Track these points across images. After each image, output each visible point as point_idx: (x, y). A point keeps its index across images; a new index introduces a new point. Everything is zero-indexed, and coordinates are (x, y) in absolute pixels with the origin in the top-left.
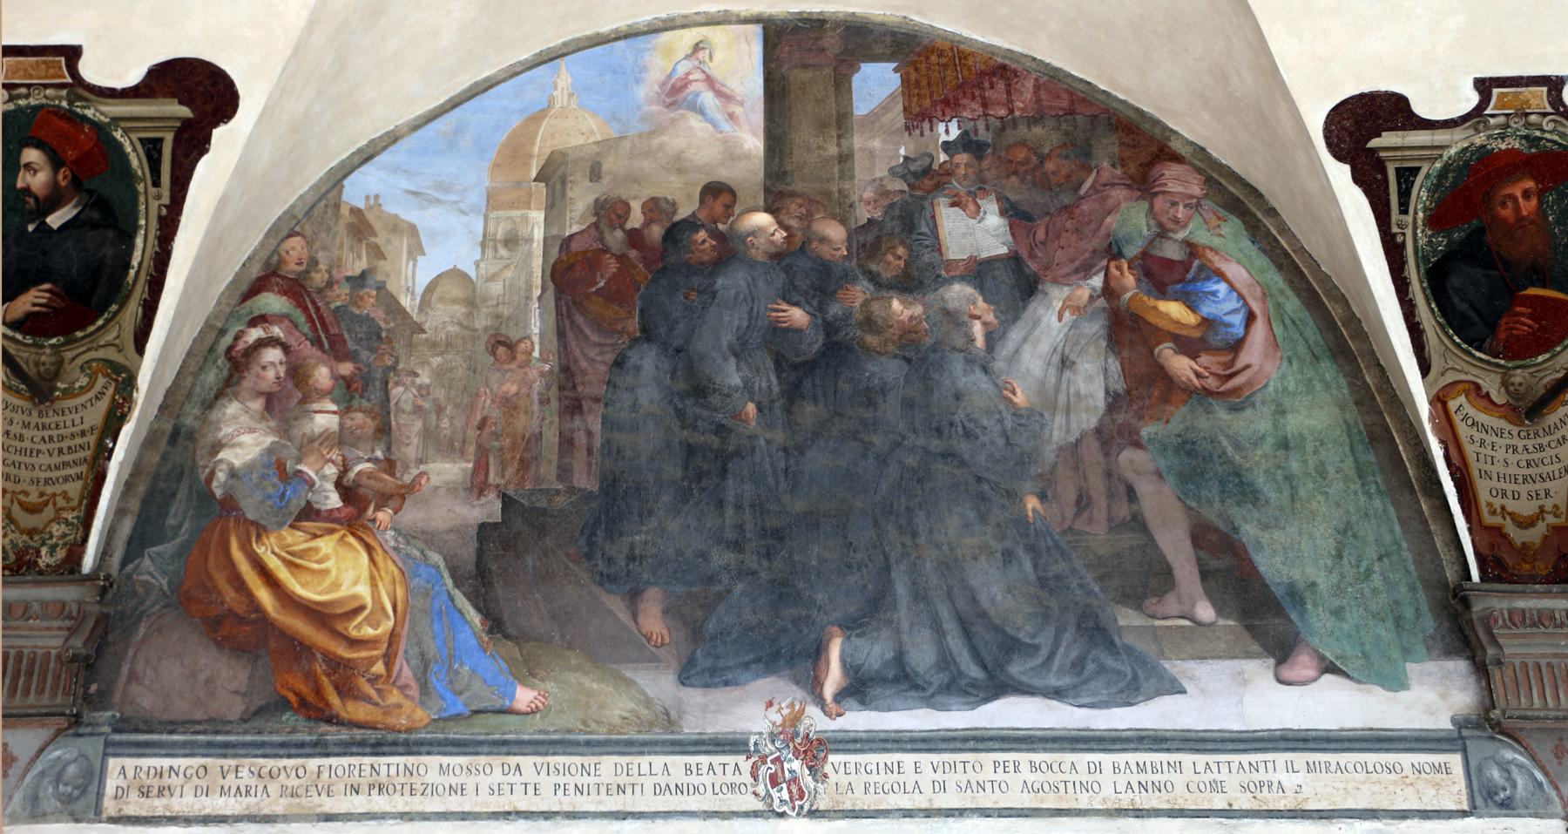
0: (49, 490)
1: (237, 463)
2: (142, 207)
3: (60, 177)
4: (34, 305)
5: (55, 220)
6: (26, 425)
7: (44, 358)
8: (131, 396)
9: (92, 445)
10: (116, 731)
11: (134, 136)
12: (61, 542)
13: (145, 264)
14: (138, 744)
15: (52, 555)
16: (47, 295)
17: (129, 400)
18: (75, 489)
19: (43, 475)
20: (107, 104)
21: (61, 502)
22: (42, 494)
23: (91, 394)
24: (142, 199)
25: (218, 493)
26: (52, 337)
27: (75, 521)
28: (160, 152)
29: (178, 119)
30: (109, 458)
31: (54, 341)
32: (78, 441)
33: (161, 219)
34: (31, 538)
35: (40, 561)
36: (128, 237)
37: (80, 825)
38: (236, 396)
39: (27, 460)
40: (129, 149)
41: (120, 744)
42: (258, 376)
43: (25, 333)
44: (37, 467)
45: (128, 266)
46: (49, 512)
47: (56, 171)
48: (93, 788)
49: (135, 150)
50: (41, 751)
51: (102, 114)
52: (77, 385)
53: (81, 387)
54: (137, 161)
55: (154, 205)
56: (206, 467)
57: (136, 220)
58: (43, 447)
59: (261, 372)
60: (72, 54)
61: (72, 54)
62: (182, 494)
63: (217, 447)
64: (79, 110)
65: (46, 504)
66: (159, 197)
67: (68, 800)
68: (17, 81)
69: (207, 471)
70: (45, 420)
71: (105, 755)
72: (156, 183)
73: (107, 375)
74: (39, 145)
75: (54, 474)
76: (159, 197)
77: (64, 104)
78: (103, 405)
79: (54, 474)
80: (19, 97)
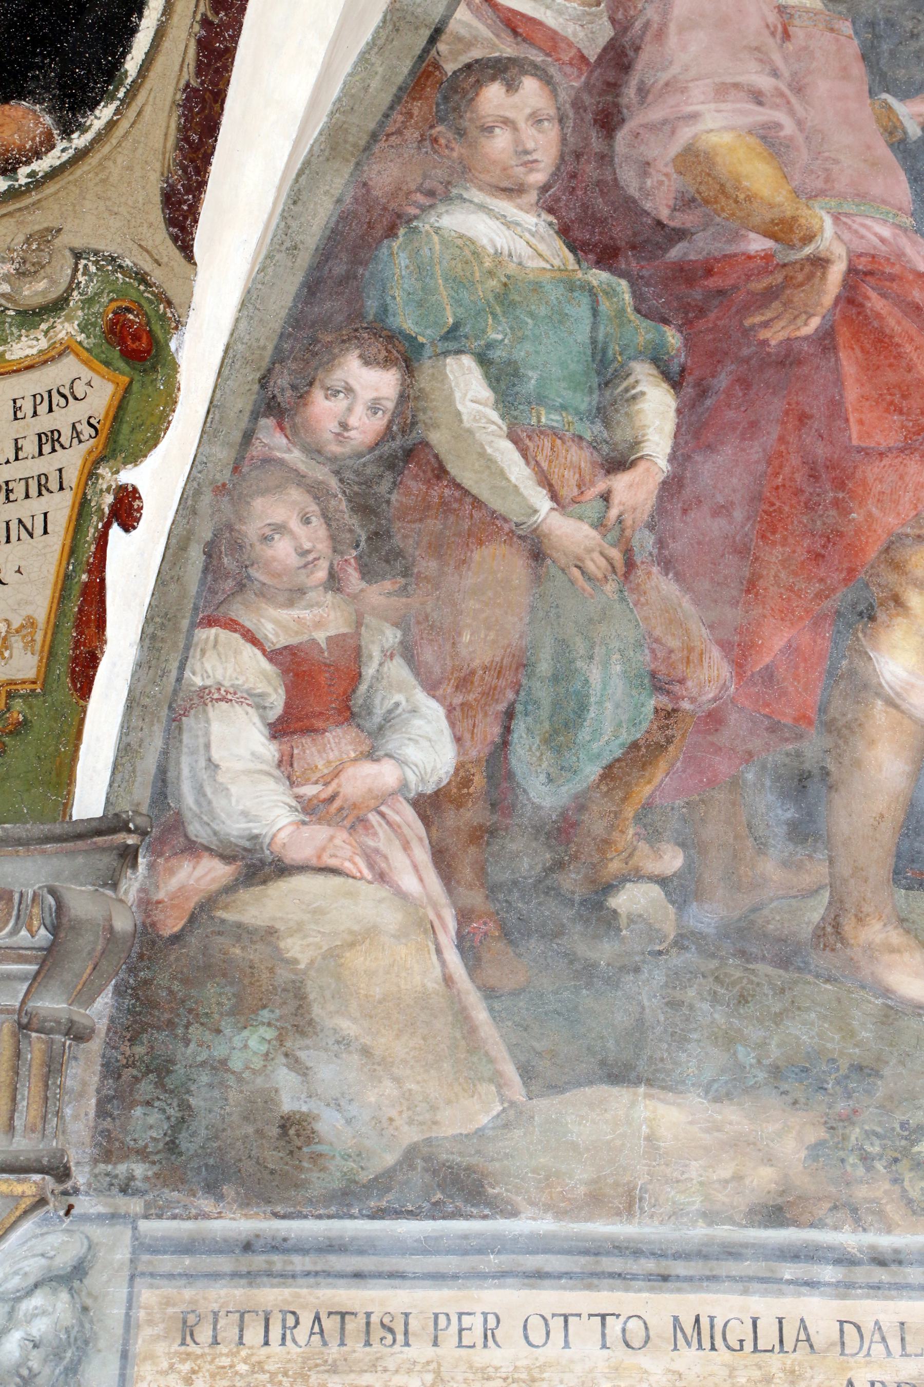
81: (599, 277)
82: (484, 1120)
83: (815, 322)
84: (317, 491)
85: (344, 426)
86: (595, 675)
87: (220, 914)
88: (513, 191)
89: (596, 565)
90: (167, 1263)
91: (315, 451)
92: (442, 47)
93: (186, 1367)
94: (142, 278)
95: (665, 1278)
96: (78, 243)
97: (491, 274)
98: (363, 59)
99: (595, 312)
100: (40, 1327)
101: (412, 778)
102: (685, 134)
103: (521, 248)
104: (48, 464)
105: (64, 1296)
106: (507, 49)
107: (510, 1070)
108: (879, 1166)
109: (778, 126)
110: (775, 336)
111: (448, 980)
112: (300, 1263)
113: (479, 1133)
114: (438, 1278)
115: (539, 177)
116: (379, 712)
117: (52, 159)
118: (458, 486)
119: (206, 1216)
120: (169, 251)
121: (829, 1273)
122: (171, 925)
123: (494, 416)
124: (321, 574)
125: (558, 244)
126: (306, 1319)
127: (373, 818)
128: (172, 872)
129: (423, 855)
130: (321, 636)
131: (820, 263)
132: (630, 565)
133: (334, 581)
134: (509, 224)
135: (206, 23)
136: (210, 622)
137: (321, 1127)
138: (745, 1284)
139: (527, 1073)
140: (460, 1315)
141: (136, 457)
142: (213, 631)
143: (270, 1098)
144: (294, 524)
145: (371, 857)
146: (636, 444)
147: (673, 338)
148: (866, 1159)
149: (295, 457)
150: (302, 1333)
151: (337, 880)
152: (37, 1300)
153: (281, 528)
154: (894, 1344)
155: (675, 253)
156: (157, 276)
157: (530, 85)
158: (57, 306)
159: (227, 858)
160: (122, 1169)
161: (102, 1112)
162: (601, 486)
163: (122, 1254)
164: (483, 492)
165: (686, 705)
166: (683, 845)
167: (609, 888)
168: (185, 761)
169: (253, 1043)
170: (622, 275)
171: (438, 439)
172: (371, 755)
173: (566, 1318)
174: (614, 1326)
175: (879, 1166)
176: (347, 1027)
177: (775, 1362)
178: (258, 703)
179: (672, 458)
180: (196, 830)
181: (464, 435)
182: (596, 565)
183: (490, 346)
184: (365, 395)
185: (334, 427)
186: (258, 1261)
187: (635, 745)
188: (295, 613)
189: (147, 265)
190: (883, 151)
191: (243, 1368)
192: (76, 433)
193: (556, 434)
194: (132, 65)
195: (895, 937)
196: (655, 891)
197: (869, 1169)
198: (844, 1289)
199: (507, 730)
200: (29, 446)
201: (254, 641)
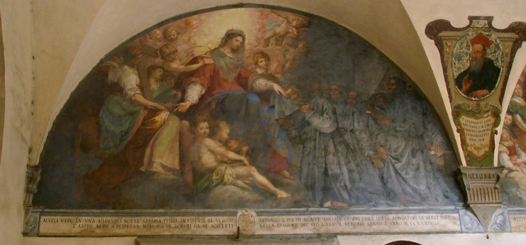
60: (490, 19)
87: (508, 176)
88: (519, 96)
94: (497, 108)
97: (519, 105)
100: (500, 219)
104: (488, 128)
105: (502, 216)
117: (488, 96)
119: (514, 208)
120: (500, 105)
123: (522, 121)
127: (521, 165)
133: (511, 139)
135: (504, 82)
143: (517, 195)
151: (518, 172)
152: (499, 216)
156: (498, 108)
158: (488, 111)
168: (500, 158)
169: (514, 189)
171: (517, 123)
172: (519, 158)
178: (506, 153)
181: (520, 123)
184: (509, 118)
189: (497, 106)
194: (496, 86)
200: (486, 126)
201: (504, 145)
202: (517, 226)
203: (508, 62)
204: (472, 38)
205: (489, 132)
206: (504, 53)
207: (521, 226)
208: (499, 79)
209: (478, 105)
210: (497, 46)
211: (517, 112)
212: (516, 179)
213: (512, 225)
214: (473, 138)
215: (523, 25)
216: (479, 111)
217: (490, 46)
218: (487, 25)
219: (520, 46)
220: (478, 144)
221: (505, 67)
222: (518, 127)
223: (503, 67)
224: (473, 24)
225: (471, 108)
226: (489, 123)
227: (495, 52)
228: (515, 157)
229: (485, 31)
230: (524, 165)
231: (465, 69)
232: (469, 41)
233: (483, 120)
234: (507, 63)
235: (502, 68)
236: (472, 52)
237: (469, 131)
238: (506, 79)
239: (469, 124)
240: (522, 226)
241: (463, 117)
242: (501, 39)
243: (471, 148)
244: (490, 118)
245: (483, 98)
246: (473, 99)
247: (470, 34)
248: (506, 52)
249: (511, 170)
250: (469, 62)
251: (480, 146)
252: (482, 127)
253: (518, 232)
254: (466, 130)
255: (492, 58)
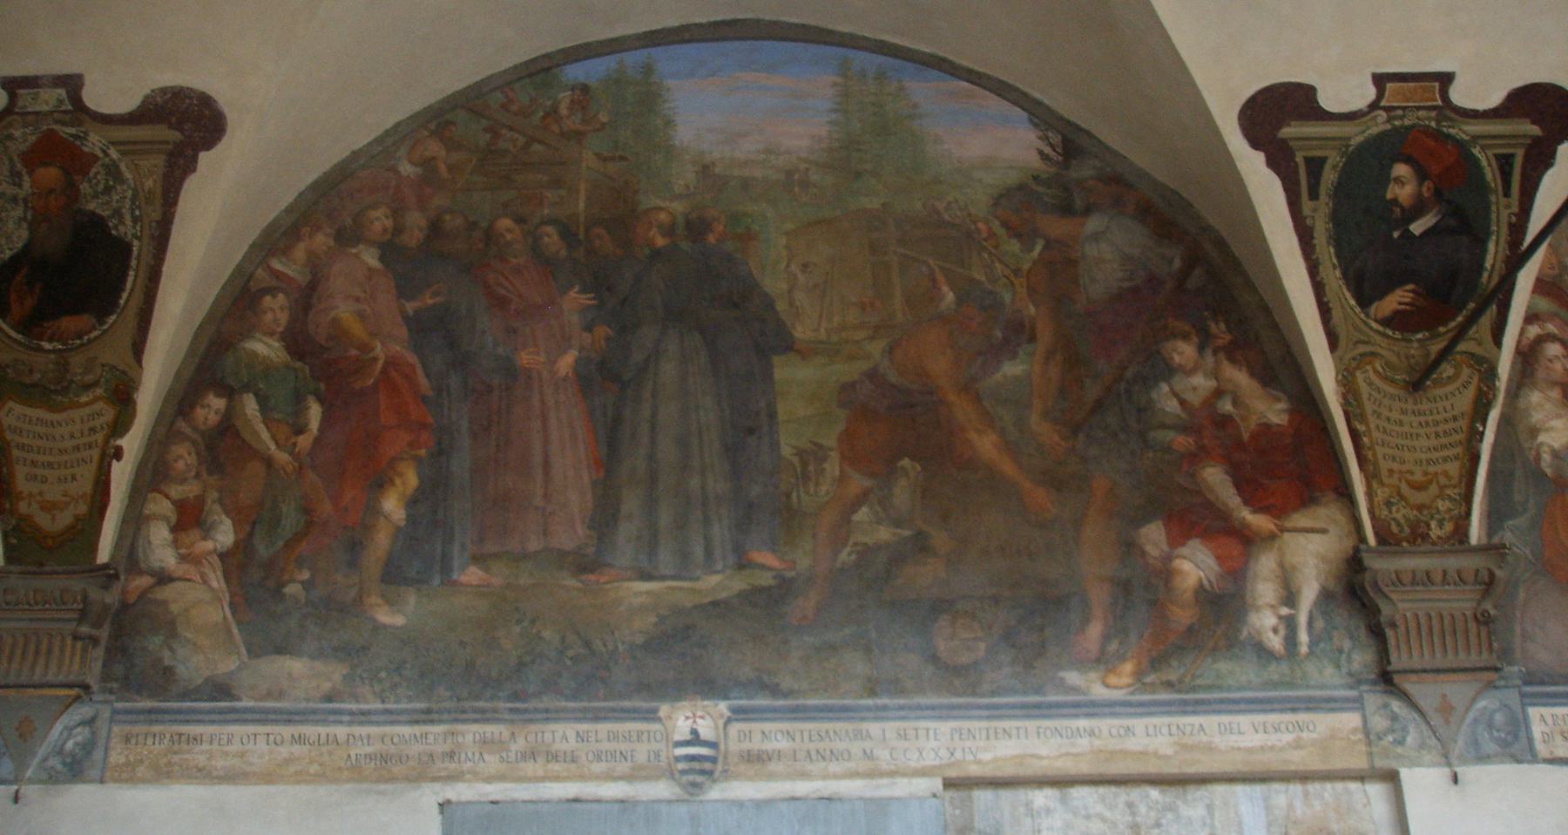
0: (1432, 469)
1: (1556, 445)
2: (1494, 216)
3: (1424, 189)
4: (1400, 304)
5: (1417, 228)
6: (1404, 412)
7: (1413, 352)
8: (1494, 385)
9: (1464, 429)
10: (1528, 683)
11: (1490, 153)
12: (1447, 516)
13: (1497, 267)
14: (1547, 695)
15: (1441, 528)
16: (1411, 295)
17: (1493, 388)
18: (1453, 468)
19: (1423, 456)
20: (1467, 124)
21: (1443, 480)
22: (1426, 473)
23: (1458, 383)
24: (1494, 208)
25: (1548, 471)
26: (1417, 332)
27: (1458, 497)
28: (1511, 166)
29: (1531, 136)
30: (1481, 440)
31: (1420, 336)
32: (1451, 425)
33: (1511, 226)
34: (1421, 513)
35: (1431, 533)
36: (1481, 243)
37: (1522, 766)
38: (1534, 385)
39: (1408, 442)
40: (1484, 163)
41: (1533, 695)
42: (1547, 368)
43: (1394, 329)
44: (1418, 449)
45: (1481, 267)
46: (1434, 489)
47: (1420, 185)
48: (1523, 734)
49: (1490, 165)
50: (1474, 700)
51: (1465, 132)
52: (1445, 375)
53: (1449, 378)
54: (1490, 174)
55: (1505, 213)
56: (1530, 449)
57: (1489, 227)
58: (1422, 431)
59: (1550, 365)
61: (1446, 79)
62: (1519, 473)
63: (1534, 432)
64: (1445, 130)
65: (1430, 482)
66: (1508, 206)
67: (1505, 744)
68: (1395, 104)
69: (1533, 453)
70: (1419, 406)
71: (1523, 706)
72: (1507, 194)
73: (1471, 366)
74: (1408, 160)
75: (1435, 455)
76: (1508, 206)
77: (1433, 124)
78: (1470, 393)
79: (1435, 455)
80: (1395, 118)
81: (299, 364)
82: (233, 667)
83: (372, 381)
84: (194, 442)
85: (206, 419)
86: (285, 509)
87: (149, 595)
88: (272, 334)
89: (290, 469)
90: (124, 717)
91: (195, 429)
92: (251, 283)
93: (125, 753)
94: (124, 373)
95: (289, 721)
96: (104, 362)
98: (223, 288)
99: (296, 377)
100: (79, 738)
101: (219, 546)
102: (333, 314)
103: (273, 355)
104: (92, 439)
105: (88, 728)
106: (274, 283)
107: (243, 650)
108: (367, 682)
109: (365, 311)
110: (358, 386)
111: (225, 618)
112: (167, 717)
113: (232, 673)
114: (213, 722)
115: (281, 329)
116: (210, 521)
117: (95, 334)
118: (244, 441)
121: (346, 718)
122: (132, 599)
123: (258, 414)
124: (193, 473)
125: (285, 353)
126: (168, 736)
127: (204, 561)
128: (134, 580)
129: (220, 574)
130: (191, 495)
131: (375, 359)
132: (301, 468)
133: (198, 476)
134: (269, 346)
135: (146, 286)
136: (154, 490)
137: (178, 671)
138: (316, 722)
139: (249, 651)
140: (220, 734)
141: (122, 435)
142: (153, 494)
143: (160, 660)
144: (186, 456)
145: (203, 575)
146: (307, 425)
147: (322, 386)
148: (362, 679)
149: (188, 431)
150: (166, 741)
151: (188, 583)
152: (79, 730)
153: (181, 457)
154: (365, 741)
155: (325, 356)
157: (281, 296)
158: (95, 384)
159: (152, 576)
160: (109, 685)
161: (104, 666)
162: (293, 440)
163: (107, 715)
164: (253, 444)
165: (316, 519)
166: (309, 569)
167: (284, 585)
168: (141, 541)
169: (157, 641)
170: (305, 363)
171: (239, 423)
172: (205, 538)
173: (255, 735)
174: (272, 737)
175: (367, 682)
176: (189, 635)
177: (324, 749)
178: (167, 520)
179: (319, 430)
180: (142, 565)
182: (290, 469)
183: (260, 389)
185: (202, 419)
186: (153, 717)
187: (296, 534)
188: (182, 487)
190: (400, 319)
191: (146, 753)
192: (102, 428)
193: (279, 421)
194: (122, 302)
195: (380, 601)
196: (299, 586)
197: (363, 683)
198: (350, 723)
199: (253, 528)
200: (86, 432)
201: (167, 496)
202: (127, 764)
203: (158, 222)
204: (23, 147)
205: (96, 453)
206: (141, 194)
207: (141, 761)
208: (130, 280)
209: (63, 366)
210: (113, 171)
211: (246, 388)
212: (174, 608)
213: (112, 759)
214: (40, 472)
215: (191, 98)
216: (65, 384)
217: (89, 170)
218: (67, 102)
219: (190, 167)
220: (53, 493)
221: (146, 240)
222: (237, 434)
223: (139, 239)
224: (20, 103)
225: (37, 376)
226: (97, 423)
227: (108, 190)
228: (194, 534)
229: (63, 123)
230: (216, 560)
231: (15, 251)
232: (15, 158)
233: (76, 414)
234: (154, 224)
235: (136, 243)
236: (34, 194)
237: (30, 449)
238: (154, 276)
239: (26, 426)
240: (146, 763)
241: (11, 404)
242: (122, 148)
243: (30, 504)
244: (100, 405)
245: (78, 342)
246: (47, 345)
247: (17, 133)
248: (146, 189)
249: (163, 578)
250: (25, 225)
251: (63, 499)
252: (72, 436)
253: (126, 781)
254: (18, 447)
255: (99, 211)
